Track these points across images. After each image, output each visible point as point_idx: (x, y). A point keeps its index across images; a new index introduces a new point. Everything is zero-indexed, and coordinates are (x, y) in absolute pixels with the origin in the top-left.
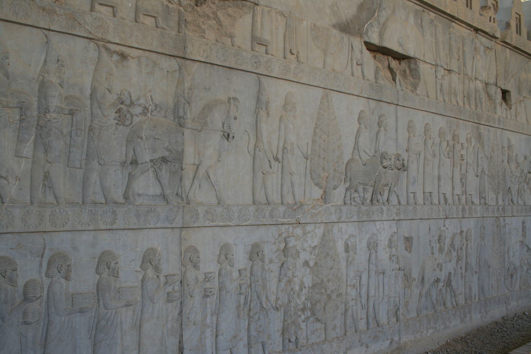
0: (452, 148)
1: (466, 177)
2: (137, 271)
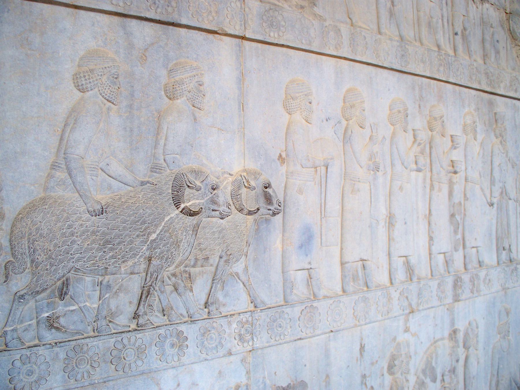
0: (428, 146)
1: (465, 210)
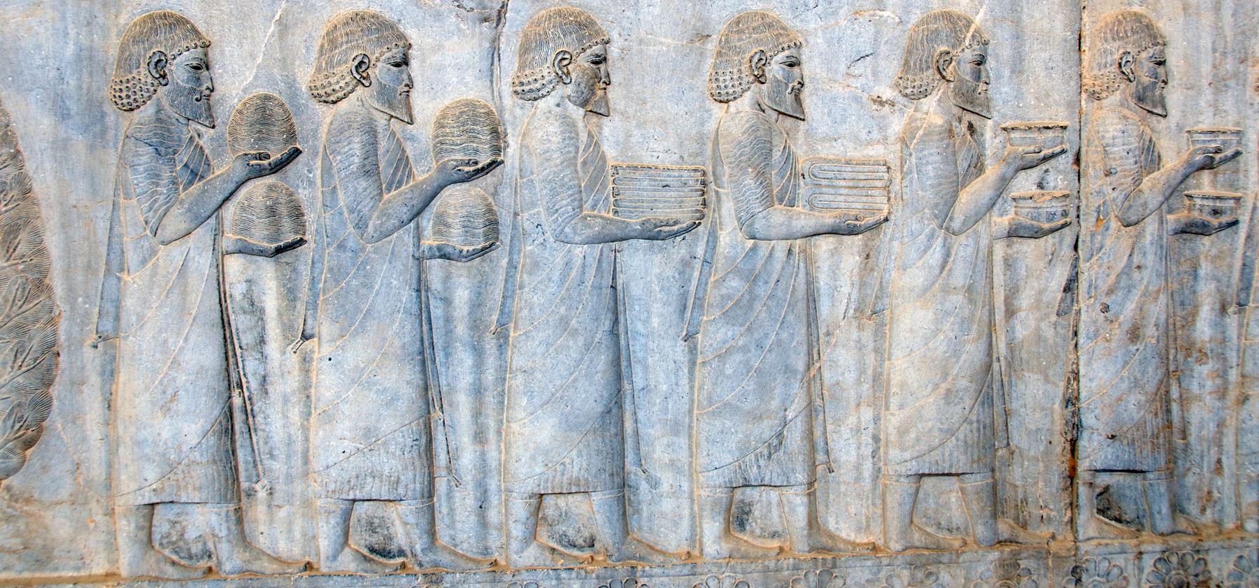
2: (879, 101)
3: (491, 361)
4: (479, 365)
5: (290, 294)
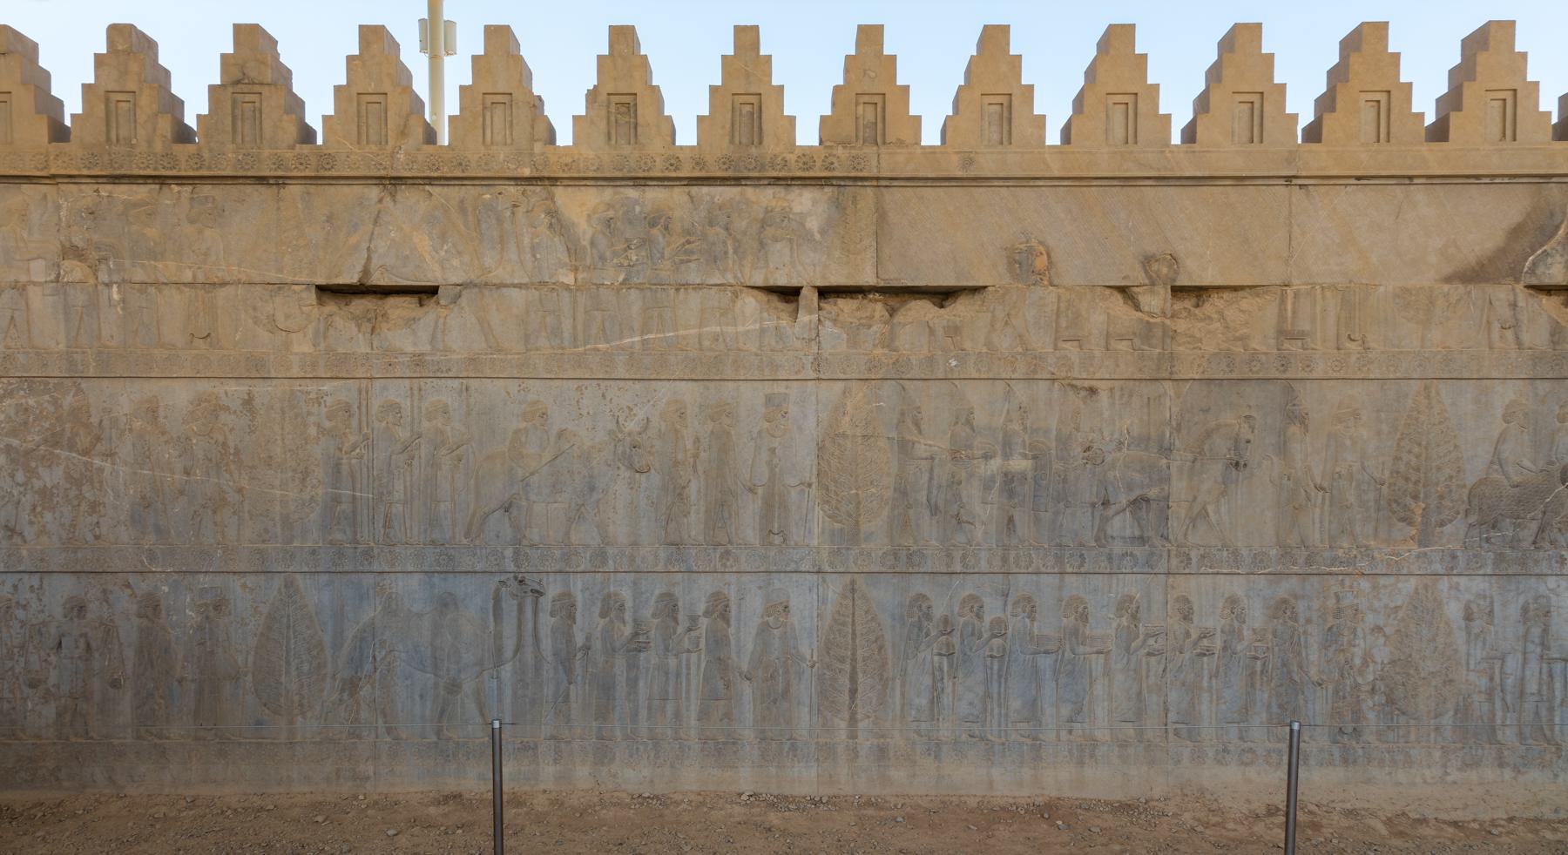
3: (1003, 685)
4: (1000, 686)
5: (951, 665)
